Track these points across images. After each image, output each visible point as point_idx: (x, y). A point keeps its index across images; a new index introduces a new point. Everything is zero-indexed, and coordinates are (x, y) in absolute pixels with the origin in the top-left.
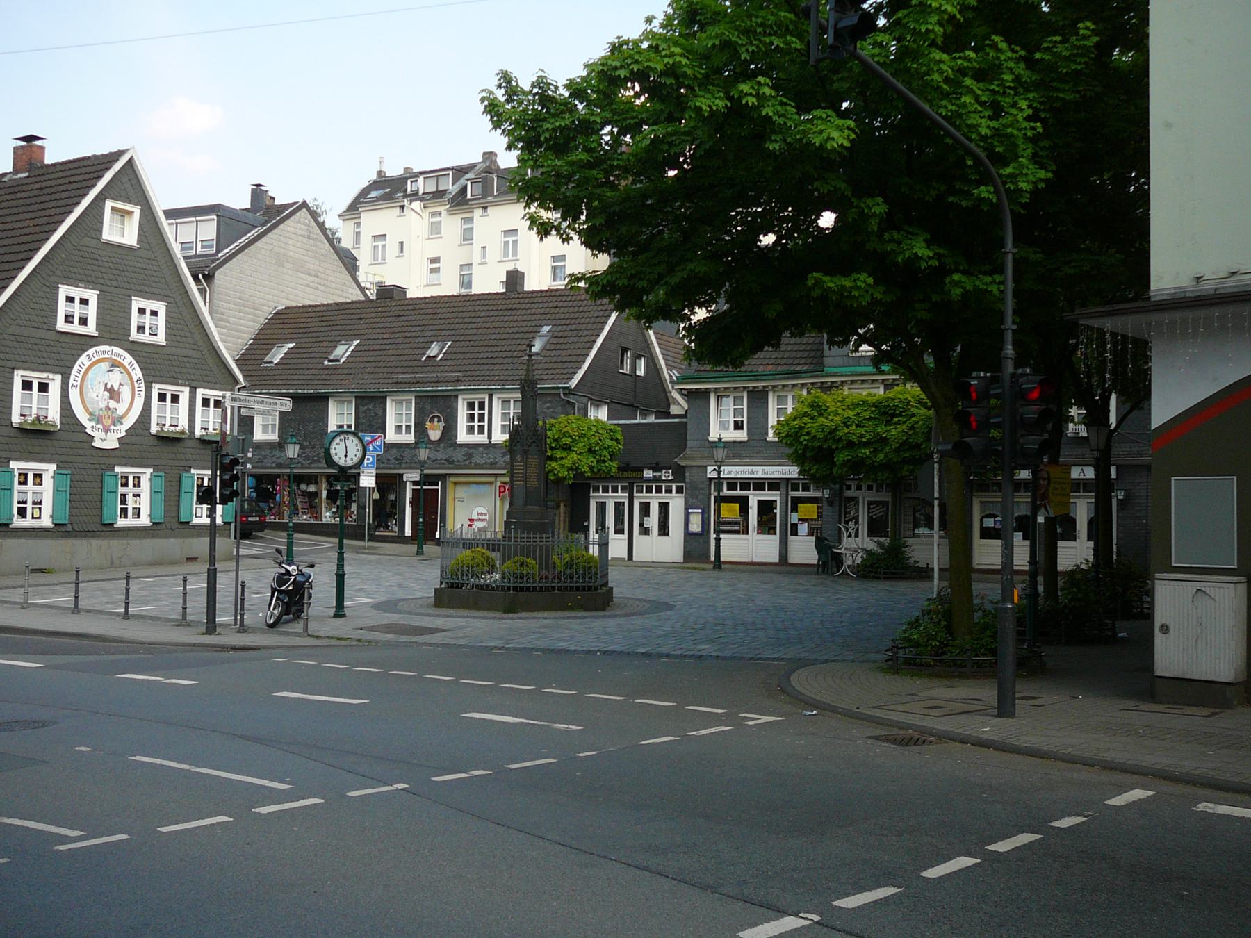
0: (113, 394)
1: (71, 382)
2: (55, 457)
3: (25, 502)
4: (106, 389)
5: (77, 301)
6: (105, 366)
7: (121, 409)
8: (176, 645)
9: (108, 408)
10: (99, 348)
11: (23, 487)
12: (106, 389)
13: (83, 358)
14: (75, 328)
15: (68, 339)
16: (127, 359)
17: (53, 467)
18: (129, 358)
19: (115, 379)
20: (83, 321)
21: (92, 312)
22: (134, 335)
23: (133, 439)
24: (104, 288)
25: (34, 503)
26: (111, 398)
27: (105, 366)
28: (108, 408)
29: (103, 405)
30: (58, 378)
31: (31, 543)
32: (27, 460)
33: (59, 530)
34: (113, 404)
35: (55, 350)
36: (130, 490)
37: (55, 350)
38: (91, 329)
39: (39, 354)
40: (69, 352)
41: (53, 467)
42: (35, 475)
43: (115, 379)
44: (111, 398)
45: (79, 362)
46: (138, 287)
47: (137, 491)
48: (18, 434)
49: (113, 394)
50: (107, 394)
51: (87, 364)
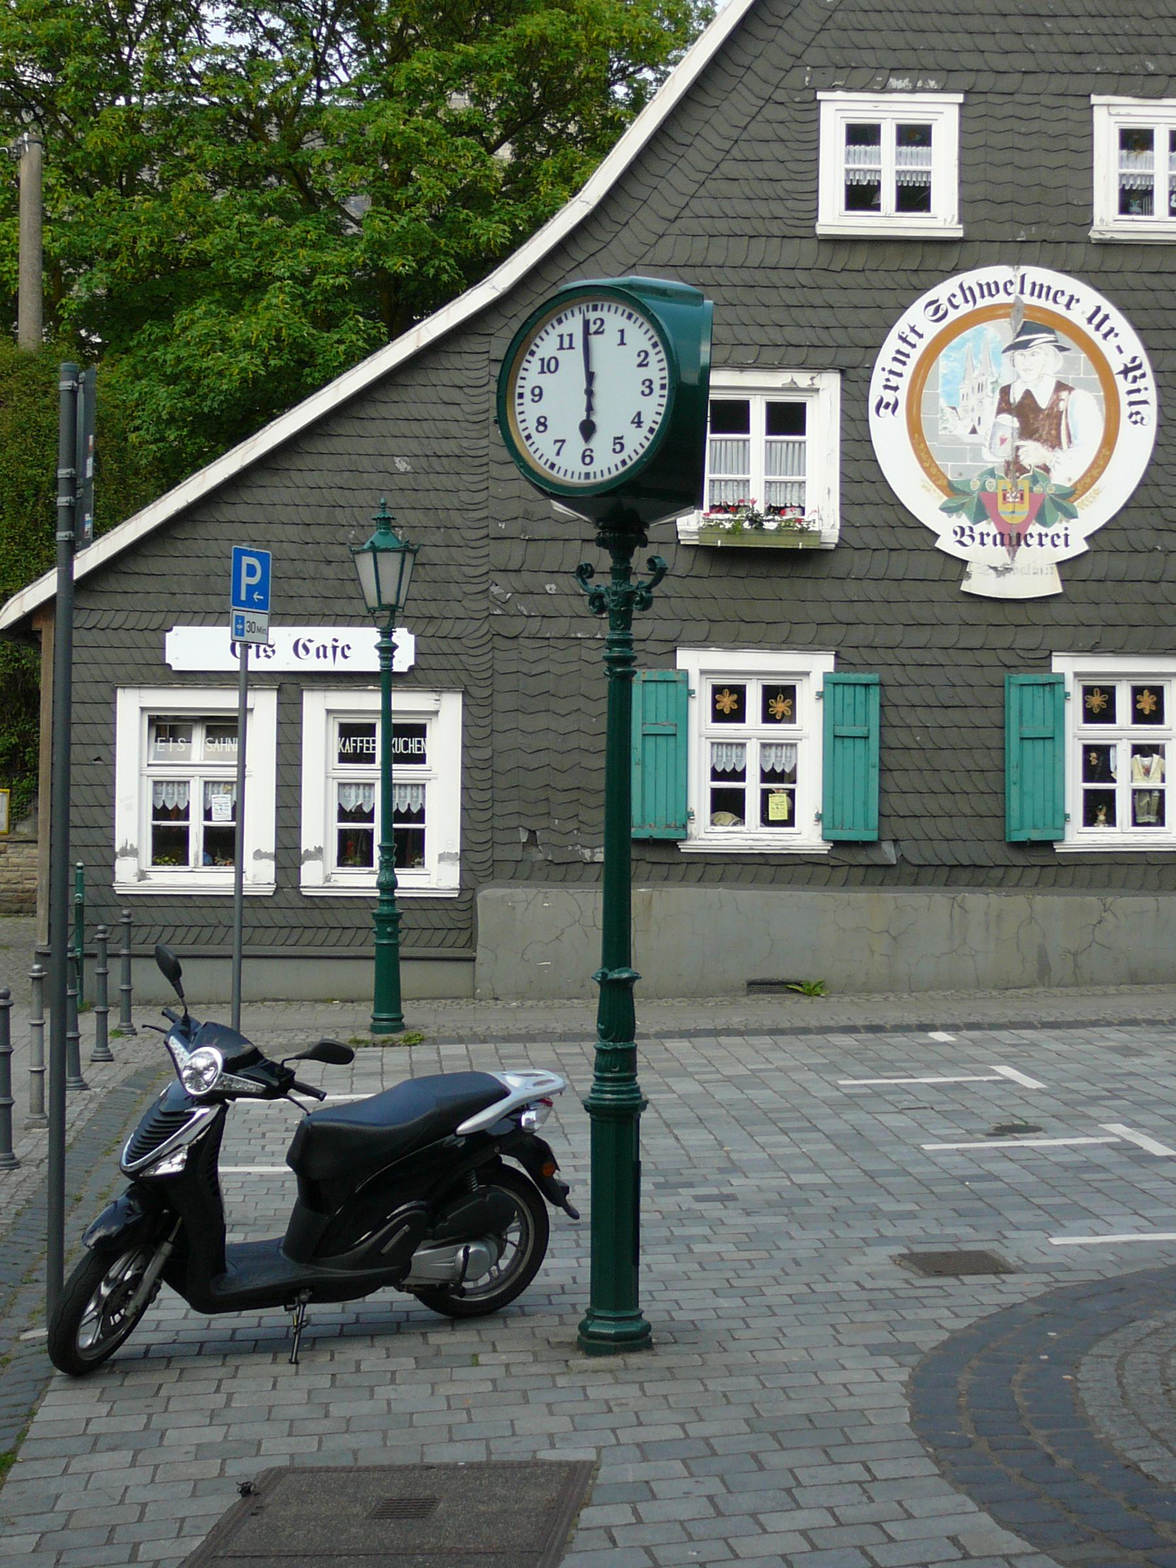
0: (1034, 419)
1: (876, 391)
2: (828, 633)
3: (740, 776)
4: (1005, 406)
5: (888, 135)
6: (998, 332)
7: (1066, 467)
8: (382, 1469)
9: (1015, 467)
10: (971, 278)
11: (728, 730)
12: (1005, 406)
13: (917, 315)
14: (887, 220)
15: (859, 259)
16: (1083, 300)
17: (825, 662)
18: (1089, 298)
19: (1038, 370)
20: (914, 197)
21: (942, 166)
22: (1107, 218)
23: (1119, 565)
24: (985, 81)
25: (769, 776)
26: (1027, 431)
27: (998, 332)
28: (1015, 467)
29: (996, 457)
30: (830, 383)
31: (747, 899)
32: (734, 643)
33: (848, 861)
34: (1033, 453)
35: (816, 298)
36: (1122, 732)
37: (816, 298)
38: (943, 217)
39: (762, 315)
40: (866, 298)
41: (825, 662)
42: (770, 693)
43: (1038, 370)
44: (1027, 431)
45: (901, 326)
46: (1113, 63)
47: (1147, 733)
48: (702, 568)
49: (1034, 419)
50: (1010, 422)
51: (932, 330)
